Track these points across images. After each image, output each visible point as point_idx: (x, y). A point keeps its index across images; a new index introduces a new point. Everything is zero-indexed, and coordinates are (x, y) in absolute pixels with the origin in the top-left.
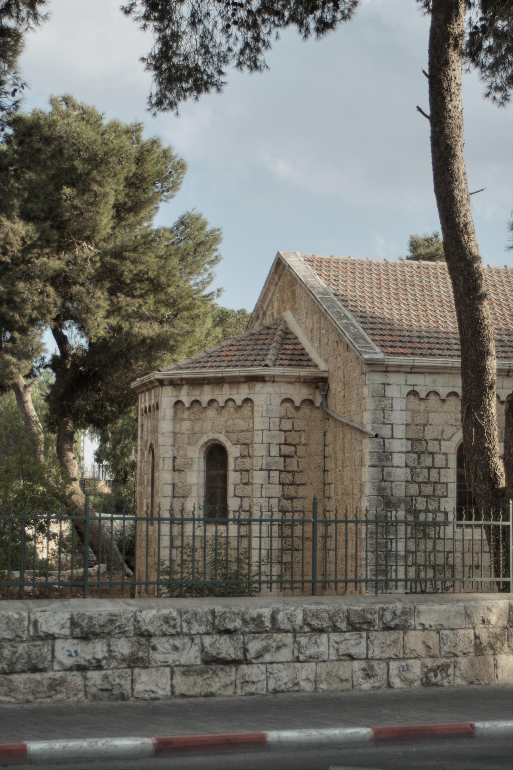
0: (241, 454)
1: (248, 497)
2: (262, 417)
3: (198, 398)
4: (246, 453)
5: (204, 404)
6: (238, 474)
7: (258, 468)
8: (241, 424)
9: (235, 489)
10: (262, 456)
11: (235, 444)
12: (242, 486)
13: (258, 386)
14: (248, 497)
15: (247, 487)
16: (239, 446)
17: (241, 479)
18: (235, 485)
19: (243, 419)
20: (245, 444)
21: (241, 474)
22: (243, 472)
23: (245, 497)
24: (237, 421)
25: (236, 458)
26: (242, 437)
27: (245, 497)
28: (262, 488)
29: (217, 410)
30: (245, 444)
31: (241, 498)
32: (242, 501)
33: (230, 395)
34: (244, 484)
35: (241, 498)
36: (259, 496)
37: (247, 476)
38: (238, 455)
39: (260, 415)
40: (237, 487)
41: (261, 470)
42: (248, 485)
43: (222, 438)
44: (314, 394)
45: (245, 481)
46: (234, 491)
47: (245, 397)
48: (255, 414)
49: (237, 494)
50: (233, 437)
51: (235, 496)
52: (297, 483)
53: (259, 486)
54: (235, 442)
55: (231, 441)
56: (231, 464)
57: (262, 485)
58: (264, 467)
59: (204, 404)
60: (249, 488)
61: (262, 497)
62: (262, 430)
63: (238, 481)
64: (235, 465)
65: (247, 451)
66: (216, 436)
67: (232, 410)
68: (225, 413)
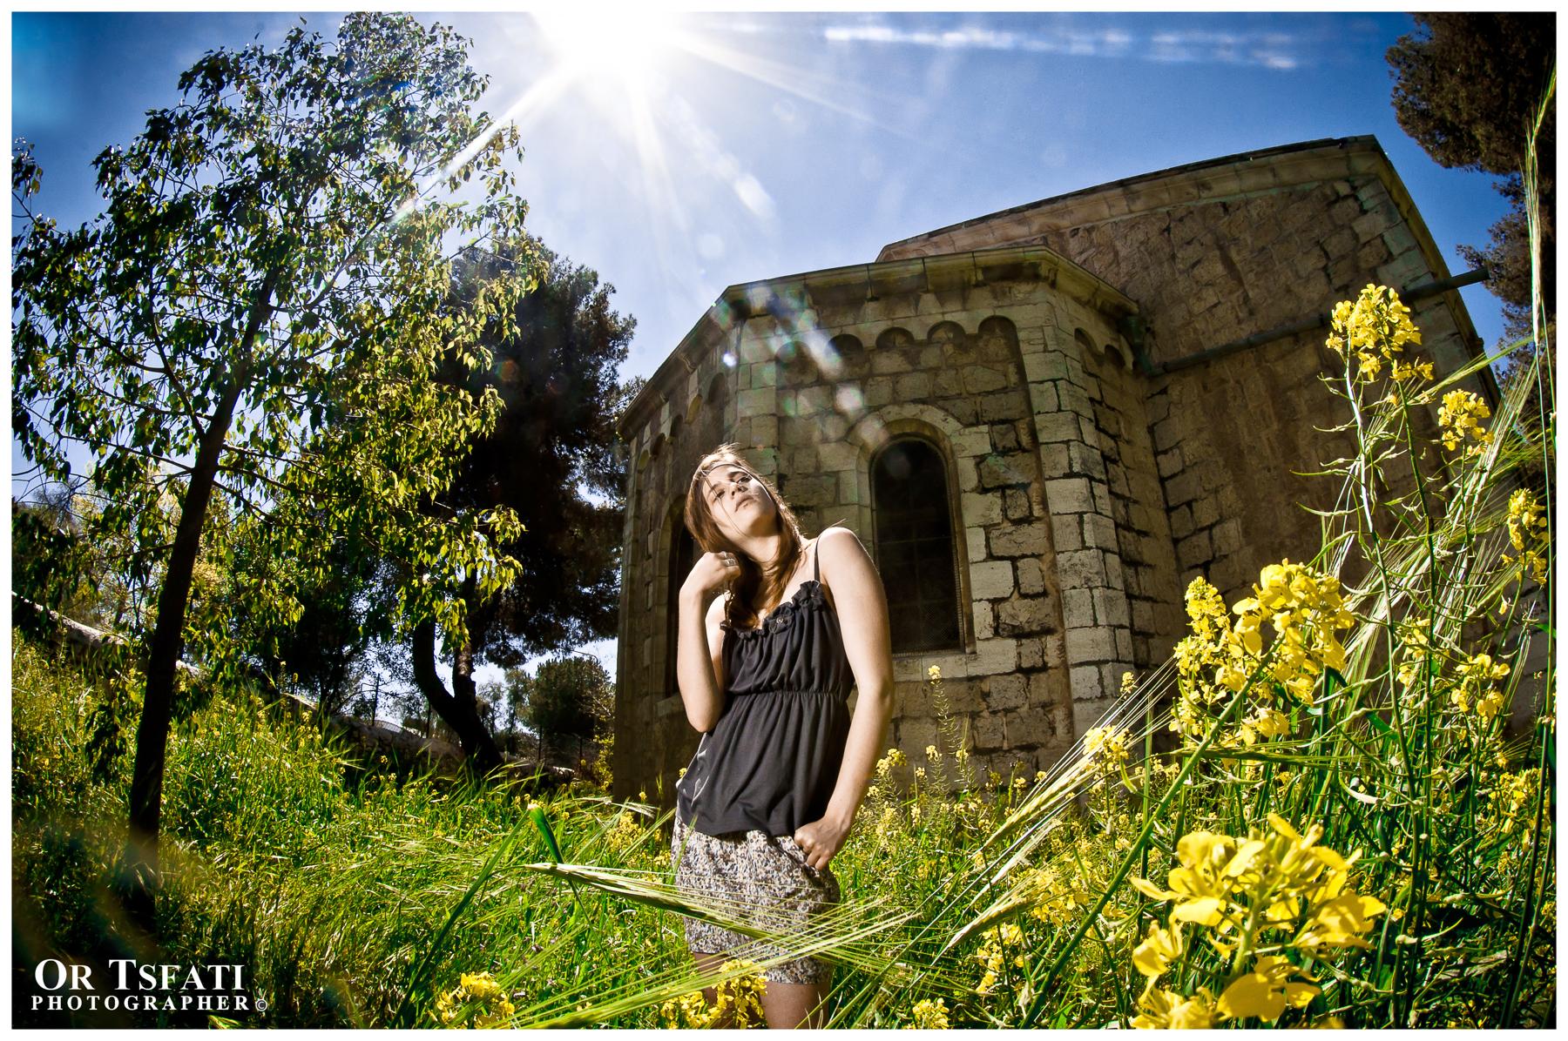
0: (994, 446)
1: (1033, 555)
2: (1045, 351)
3: (850, 331)
4: (1009, 442)
5: (869, 343)
6: (993, 499)
7: (1061, 473)
8: (984, 378)
9: (987, 540)
10: (1067, 442)
11: (972, 425)
12: (1008, 527)
13: (1021, 290)
14: (1033, 555)
15: (1026, 528)
16: (985, 428)
17: (1004, 510)
18: (988, 528)
19: (987, 363)
20: (1002, 422)
21: (1004, 497)
22: (1008, 492)
23: (1024, 556)
24: (967, 370)
25: (980, 460)
26: (993, 407)
27: (1024, 556)
28: (1081, 522)
29: (905, 353)
30: (1002, 422)
31: (1014, 560)
32: (1015, 569)
33: (943, 313)
34: (1018, 522)
35: (1014, 560)
36: (1078, 545)
37: (1024, 500)
38: (988, 449)
39: (1041, 347)
40: (995, 533)
41: (1070, 475)
42: (1030, 523)
43: (933, 416)
44: (1118, 340)
45: (1017, 515)
46: (988, 545)
47: (988, 313)
48: (1024, 347)
49: (997, 552)
50: (965, 407)
51: (991, 557)
52: (1136, 527)
53: (1073, 520)
54: (972, 419)
55: (959, 420)
56: (968, 474)
57: (1081, 515)
58: (1076, 468)
59: (869, 343)
60: (1037, 525)
61: (1084, 547)
62: (1054, 381)
63: (996, 515)
64: (980, 477)
65: (1012, 436)
66: (910, 411)
67: (949, 349)
68: (930, 357)
